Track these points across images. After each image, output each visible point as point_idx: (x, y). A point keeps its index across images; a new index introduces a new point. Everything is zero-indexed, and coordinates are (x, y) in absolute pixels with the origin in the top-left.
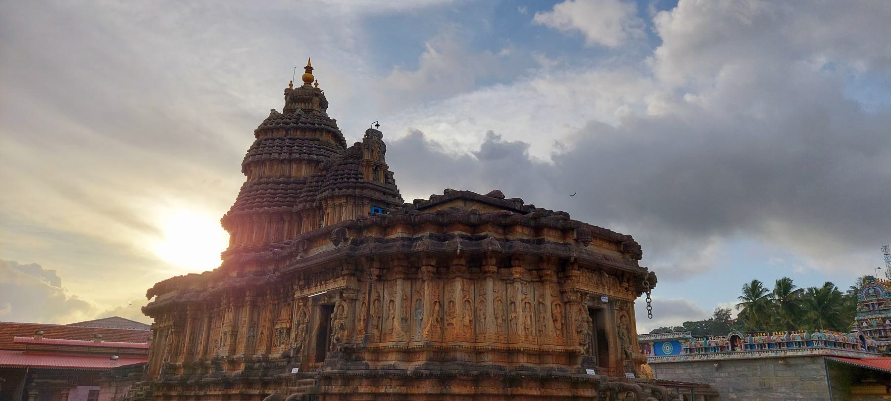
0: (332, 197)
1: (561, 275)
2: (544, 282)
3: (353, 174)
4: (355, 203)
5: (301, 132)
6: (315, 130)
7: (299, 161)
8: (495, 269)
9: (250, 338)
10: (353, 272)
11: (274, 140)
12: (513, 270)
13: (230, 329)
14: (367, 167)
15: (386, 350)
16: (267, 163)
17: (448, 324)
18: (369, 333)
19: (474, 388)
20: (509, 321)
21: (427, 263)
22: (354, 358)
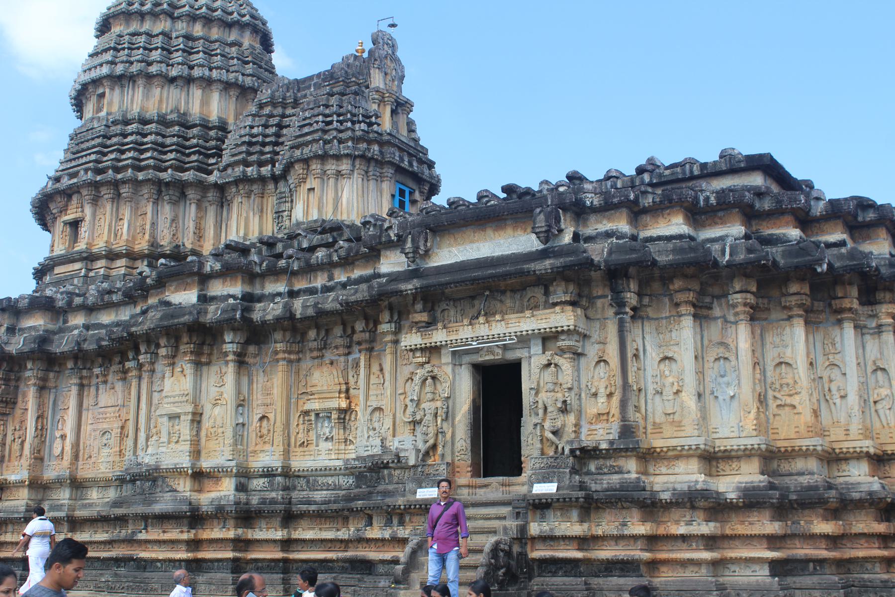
0: (323, 157)
4: (367, 172)
5: (204, 26)
6: (229, 25)
7: (208, 82)
8: (855, 304)
9: (238, 428)
10: (576, 299)
11: (149, 35)
12: (883, 310)
13: (190, 408)
14: (382, 104)
15: (670, 453)
16: (141, 82)
17: (779, 406)
18: (632, 419)
20: (872, 404)
21: (743, 288)
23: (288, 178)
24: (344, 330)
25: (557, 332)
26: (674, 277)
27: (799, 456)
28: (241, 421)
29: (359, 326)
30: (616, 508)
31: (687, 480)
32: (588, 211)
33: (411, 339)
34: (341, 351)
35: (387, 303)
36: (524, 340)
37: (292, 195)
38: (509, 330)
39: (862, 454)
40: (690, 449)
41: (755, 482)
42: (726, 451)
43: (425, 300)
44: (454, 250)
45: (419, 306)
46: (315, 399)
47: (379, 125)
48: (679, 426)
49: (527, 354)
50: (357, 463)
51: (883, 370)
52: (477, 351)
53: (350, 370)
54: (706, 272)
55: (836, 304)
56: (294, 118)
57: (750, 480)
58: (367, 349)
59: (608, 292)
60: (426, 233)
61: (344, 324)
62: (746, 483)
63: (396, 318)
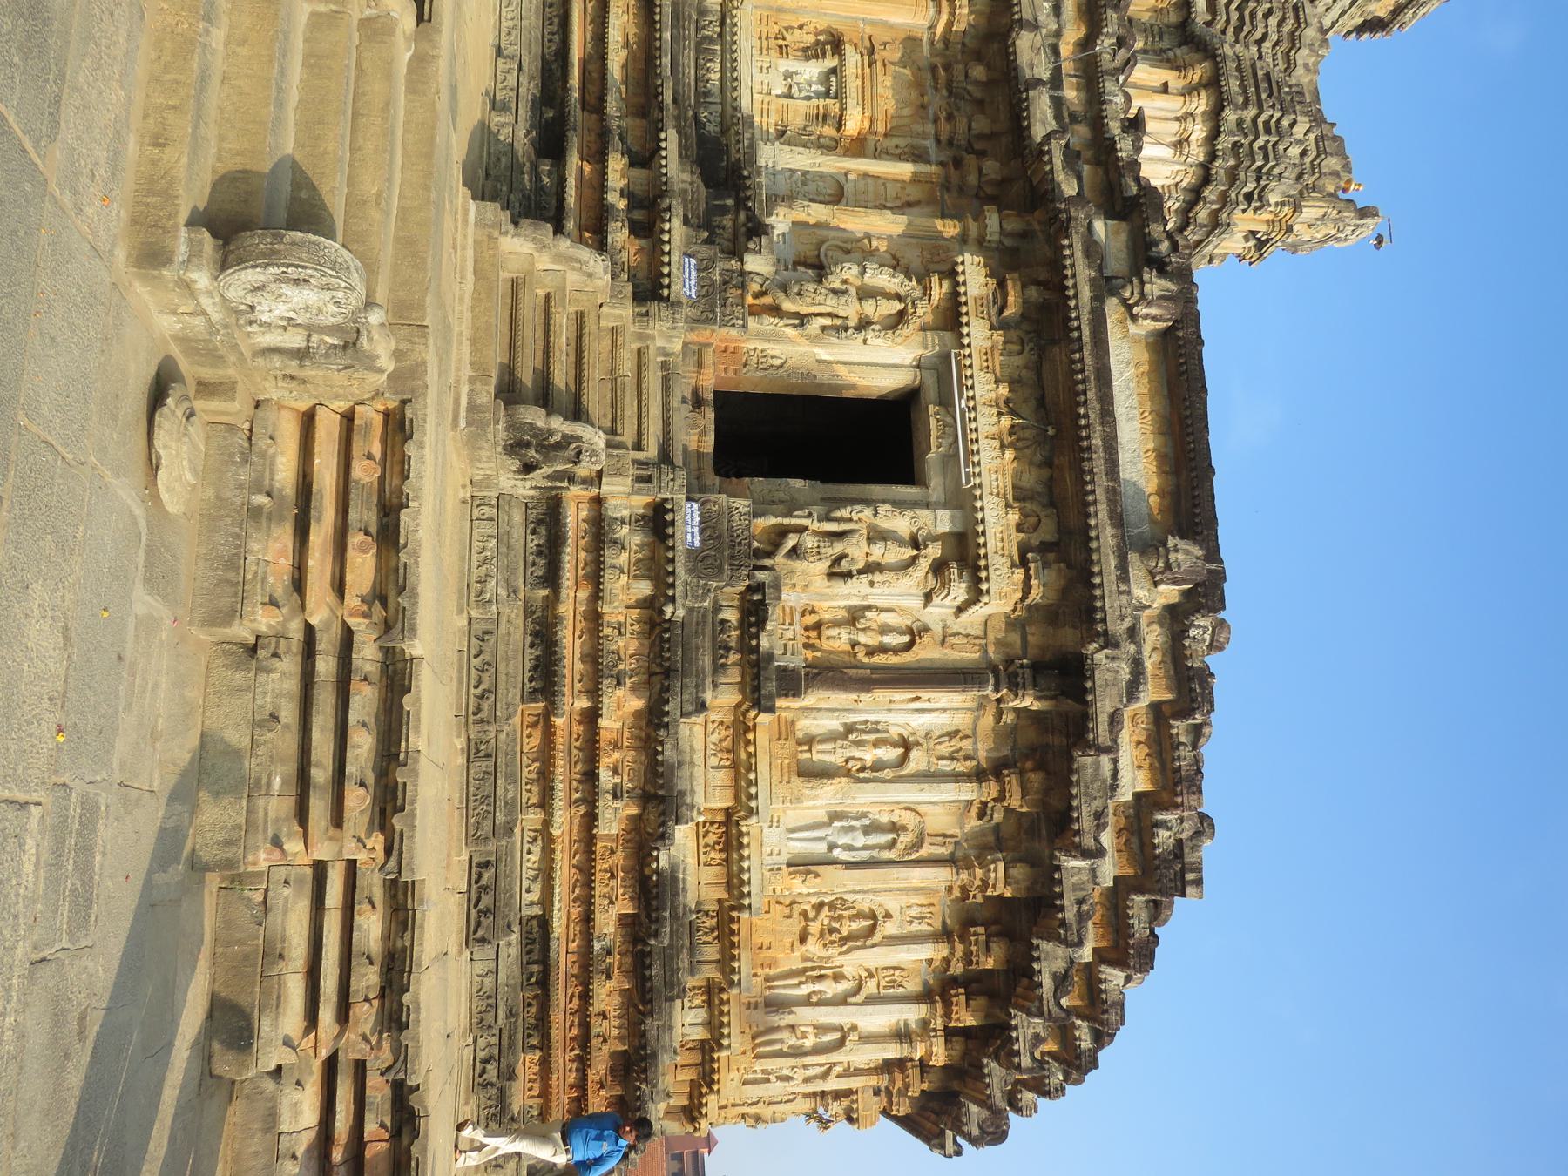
2: (886, 1076)
3: (1266, 186)
22: (721, 616)
23: (1185, 49)
24: (981, 136)
25: (978, 568)
26: (1048, 773)
27: (722, 951)
29: (991, 167)
30: (651, 661)
31: (695, 788)
32: (1177, 628)
33: (975, 276)
34: (945, 128)
35: (1037, 227)
36: (963, 501)
37: (1155, 52)
38: (985, 474)
40: (750, 797)
41: (685, 896)
42: (741, 846)
43: (1044, 307)
44: (1131, 372)
45: (1033, 293)
46: (863, 69)
47: (1244, 211)
48: (789, 772)
49: (933, 498)
50: (746, 143)
51: (841, 1043)
52: (946, 402)
53: (909, 140)
55: (957, 995)
56: (1259, 64)
57: (688, 886)
58: (947, 178)
59: (1032, 652)
60: (1169, 320)
61: (991, 136)
62: (684, 879)
63: (1008, 242)
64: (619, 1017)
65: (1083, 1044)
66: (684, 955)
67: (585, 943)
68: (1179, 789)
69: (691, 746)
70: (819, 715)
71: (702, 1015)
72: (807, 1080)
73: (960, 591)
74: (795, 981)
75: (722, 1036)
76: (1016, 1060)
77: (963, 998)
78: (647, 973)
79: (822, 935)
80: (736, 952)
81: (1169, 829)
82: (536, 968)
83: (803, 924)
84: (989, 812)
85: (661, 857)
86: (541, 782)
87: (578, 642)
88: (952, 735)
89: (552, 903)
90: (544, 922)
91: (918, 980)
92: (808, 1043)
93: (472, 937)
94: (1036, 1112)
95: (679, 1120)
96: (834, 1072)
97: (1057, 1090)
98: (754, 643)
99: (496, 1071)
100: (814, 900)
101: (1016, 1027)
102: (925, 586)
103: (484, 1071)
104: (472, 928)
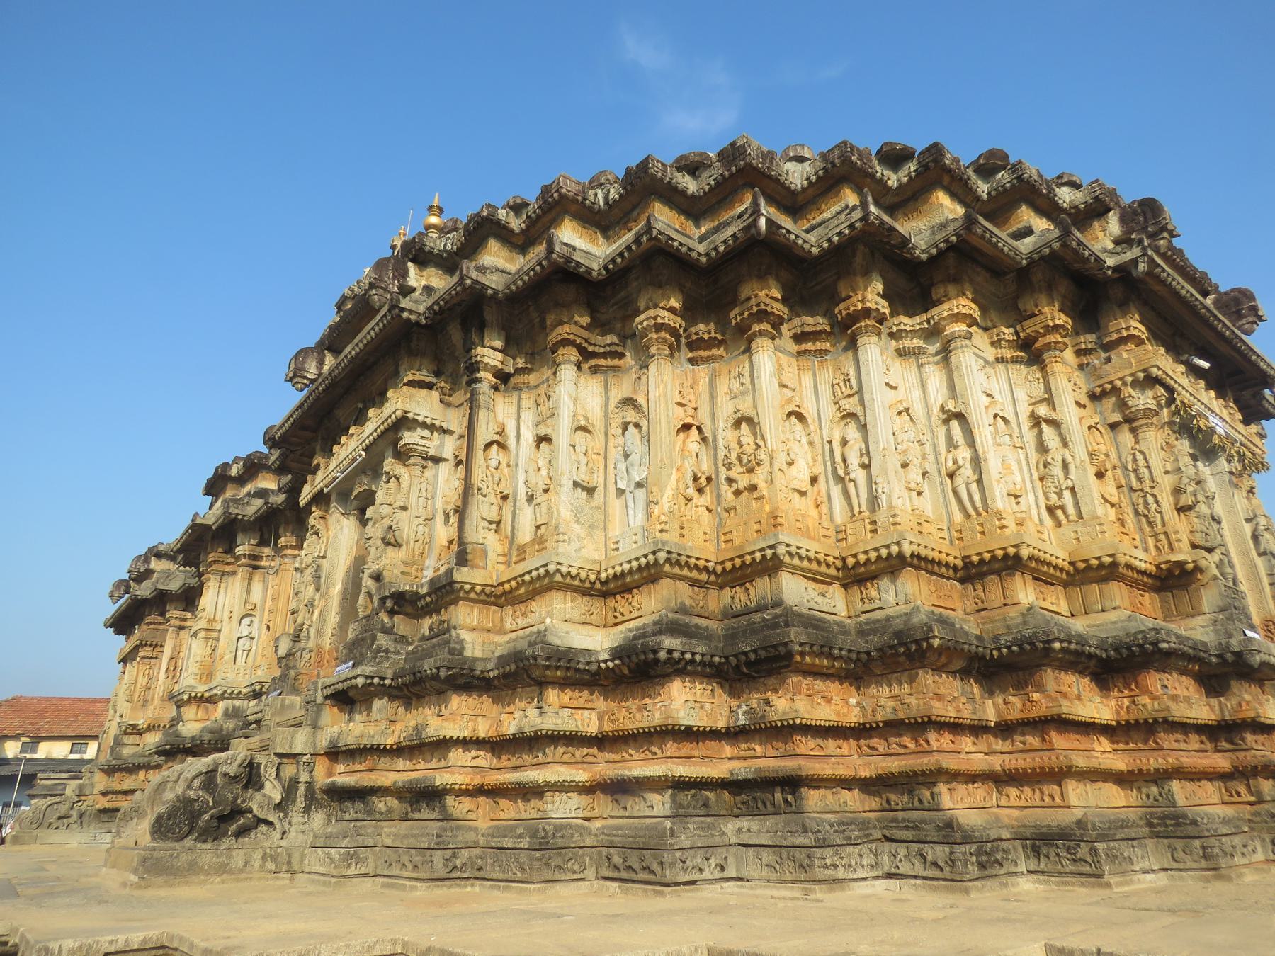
1: (1088, 340)
2: (1045, 356)
8: (884, 307)
19: (858, 704)
22: (427, 633)
27: (761, 574)
28: (245, 633)
39: (894, 562)
42: (615, 576)
51: (960, 417)
54: (613, 301)
62: (637, 629)
64: (890, 686)
65: (912, 169)
66: (757, 617)
67: (757, 737)
68: (550, 200)
69: (508, 642)
70: (516, 526)
71: (885, 583)
72: (1065, 445)
73: (409, 437)
74: (851, 486)
75: (890, 555)
76: (858, 225)
77: (842, 306)
78: (752, 656)
79: (751, 471)
80: (748, 559)
81: (609, 191)
82: (778, 796)
83: (746, 493)
84: (608, 349)
85: (601, 658)
86: (528, 796)
87: (422, 765)
88: (538, 405)
89: (648, 778)
90: (680, 785)
91: (843, 358)
92: (964, 454)
93: (658, 879)
94: (1096, 181)
95: (1198, 590)
96: (1053, 416)
97: (1013, 172)
98: (428, 599)
99: (938, 848)
100: (725, 487)
101: (829, 240)
102: (415, 464)
103: (935, 864)
104: (652, 877)
